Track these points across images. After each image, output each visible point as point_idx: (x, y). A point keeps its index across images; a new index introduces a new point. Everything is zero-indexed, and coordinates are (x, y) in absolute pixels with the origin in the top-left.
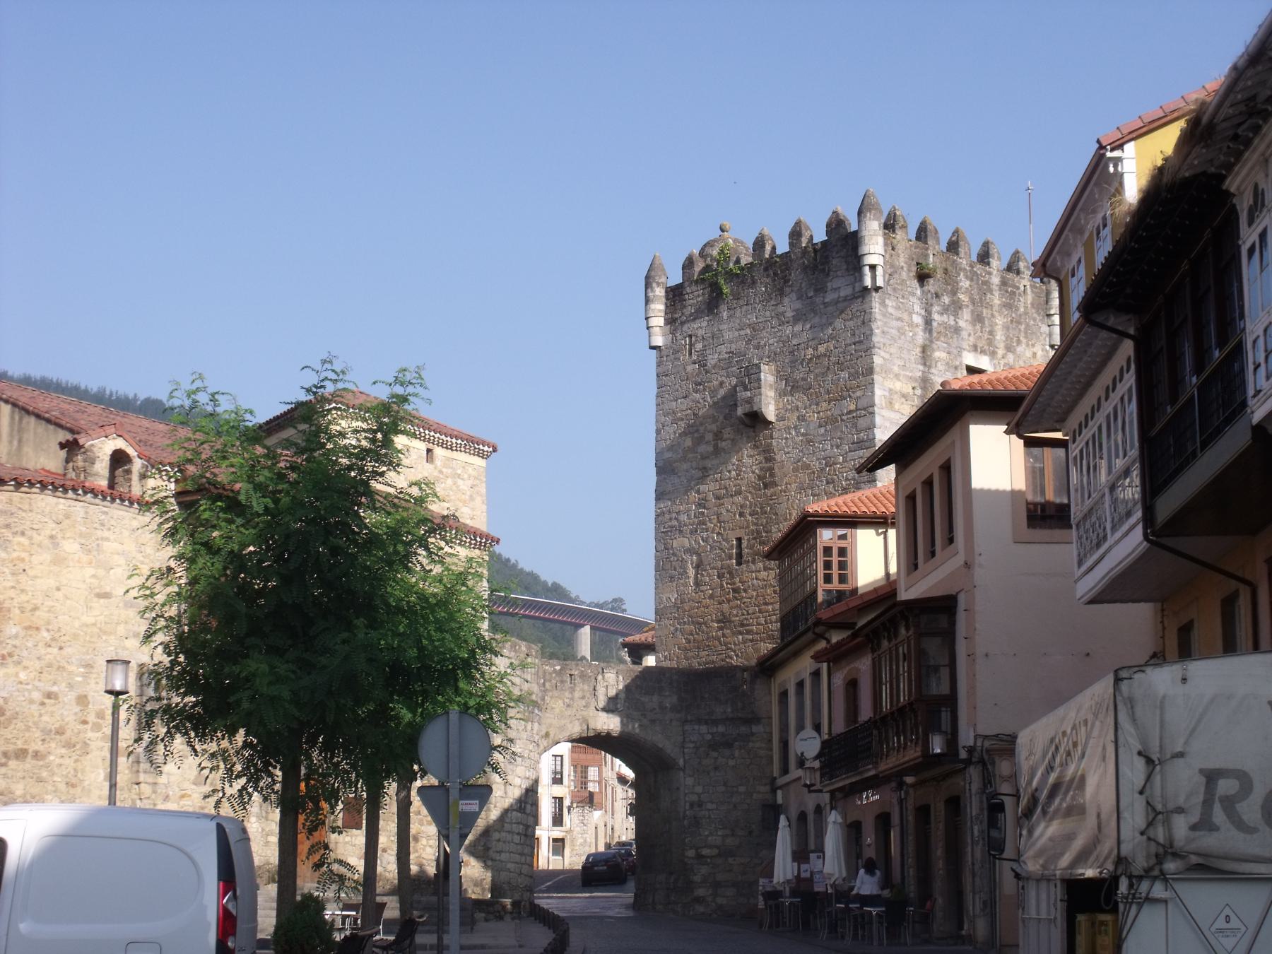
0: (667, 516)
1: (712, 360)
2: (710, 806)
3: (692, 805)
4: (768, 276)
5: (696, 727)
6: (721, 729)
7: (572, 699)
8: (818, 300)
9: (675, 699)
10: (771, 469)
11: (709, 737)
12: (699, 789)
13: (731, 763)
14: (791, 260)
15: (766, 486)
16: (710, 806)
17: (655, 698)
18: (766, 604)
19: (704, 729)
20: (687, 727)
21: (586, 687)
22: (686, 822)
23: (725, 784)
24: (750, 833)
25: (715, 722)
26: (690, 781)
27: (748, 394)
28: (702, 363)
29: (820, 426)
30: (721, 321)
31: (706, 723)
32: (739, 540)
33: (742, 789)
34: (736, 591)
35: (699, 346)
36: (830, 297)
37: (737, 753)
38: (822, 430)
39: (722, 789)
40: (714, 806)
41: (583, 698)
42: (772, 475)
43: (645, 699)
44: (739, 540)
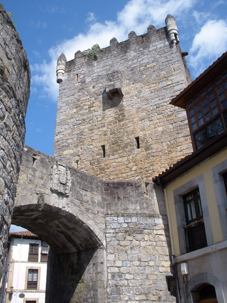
0: (61, 142)
1: (88, 80)
2: (128, 276)
3: (113, 276)
4: (118, 49)
5: (115, 218)
6: (134, 220)
7: (34, 176)
8: (146, 51)
9: (100, 199)
10: (122, 114)
11: (125, 225)
12: (119, 263)
13: (143, 244)
14: (130, 41)
15: (120, 121)
16: (128, 276)
17: (88, 194)
18: (122, 173)
19: (121, 220)
20: (107, 219)
21: (44, 171)
22: (108, 290)
23: (140, 260)
24: (159, 298)
25: (130, 216)
26: (111, 257)
27: (112, 83)
28: (83, 82)
29: (152, 93)
30: (93, 66)
31: (123, 216)
32: (103, 147)
33: (152, 263)
34: (103, 169)
35: (82, 77)
36: (150, 49)
37: (146, 237)
38: (153, 94)
39: (138, 263)
40: (132, 276)
41: (42, 178)
42: (124, 116)
43: (84, 193)
44: (103, 147)
